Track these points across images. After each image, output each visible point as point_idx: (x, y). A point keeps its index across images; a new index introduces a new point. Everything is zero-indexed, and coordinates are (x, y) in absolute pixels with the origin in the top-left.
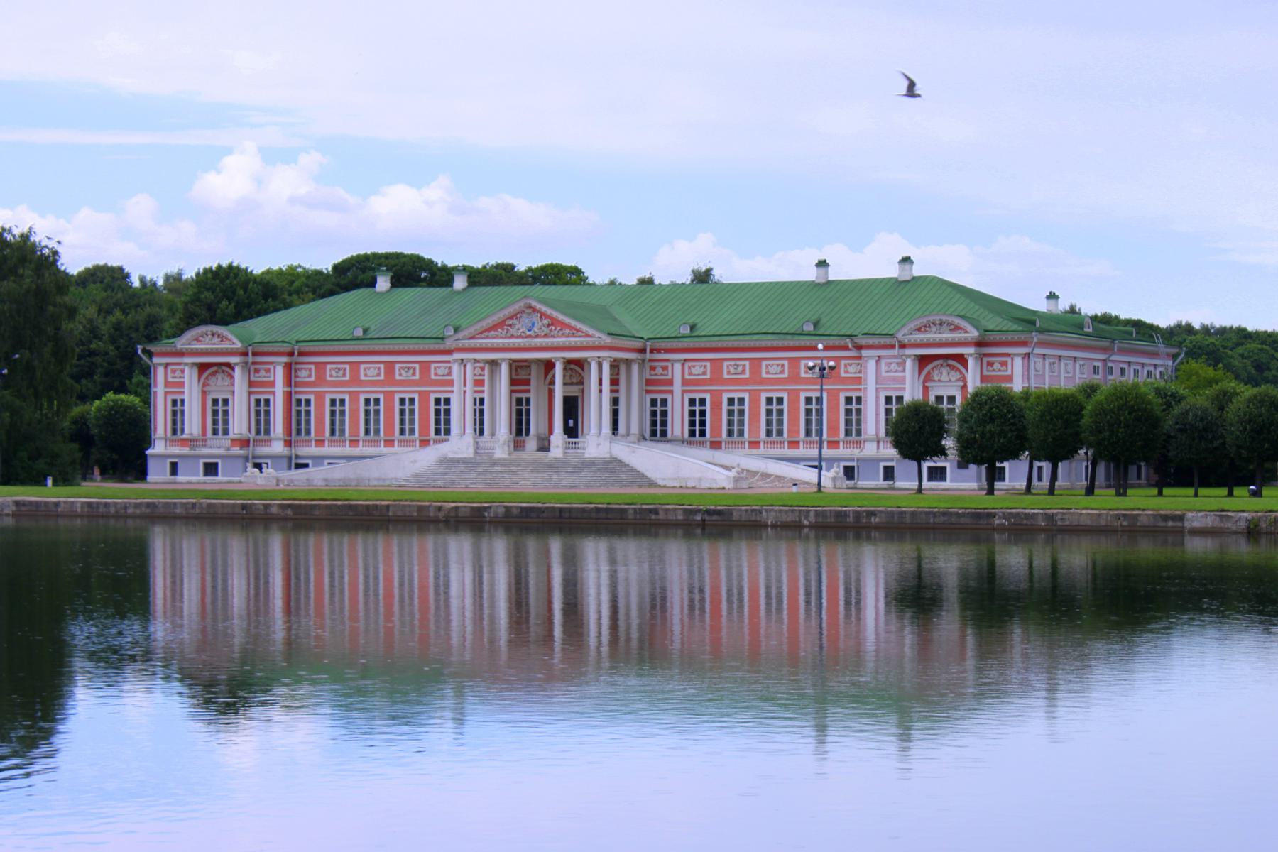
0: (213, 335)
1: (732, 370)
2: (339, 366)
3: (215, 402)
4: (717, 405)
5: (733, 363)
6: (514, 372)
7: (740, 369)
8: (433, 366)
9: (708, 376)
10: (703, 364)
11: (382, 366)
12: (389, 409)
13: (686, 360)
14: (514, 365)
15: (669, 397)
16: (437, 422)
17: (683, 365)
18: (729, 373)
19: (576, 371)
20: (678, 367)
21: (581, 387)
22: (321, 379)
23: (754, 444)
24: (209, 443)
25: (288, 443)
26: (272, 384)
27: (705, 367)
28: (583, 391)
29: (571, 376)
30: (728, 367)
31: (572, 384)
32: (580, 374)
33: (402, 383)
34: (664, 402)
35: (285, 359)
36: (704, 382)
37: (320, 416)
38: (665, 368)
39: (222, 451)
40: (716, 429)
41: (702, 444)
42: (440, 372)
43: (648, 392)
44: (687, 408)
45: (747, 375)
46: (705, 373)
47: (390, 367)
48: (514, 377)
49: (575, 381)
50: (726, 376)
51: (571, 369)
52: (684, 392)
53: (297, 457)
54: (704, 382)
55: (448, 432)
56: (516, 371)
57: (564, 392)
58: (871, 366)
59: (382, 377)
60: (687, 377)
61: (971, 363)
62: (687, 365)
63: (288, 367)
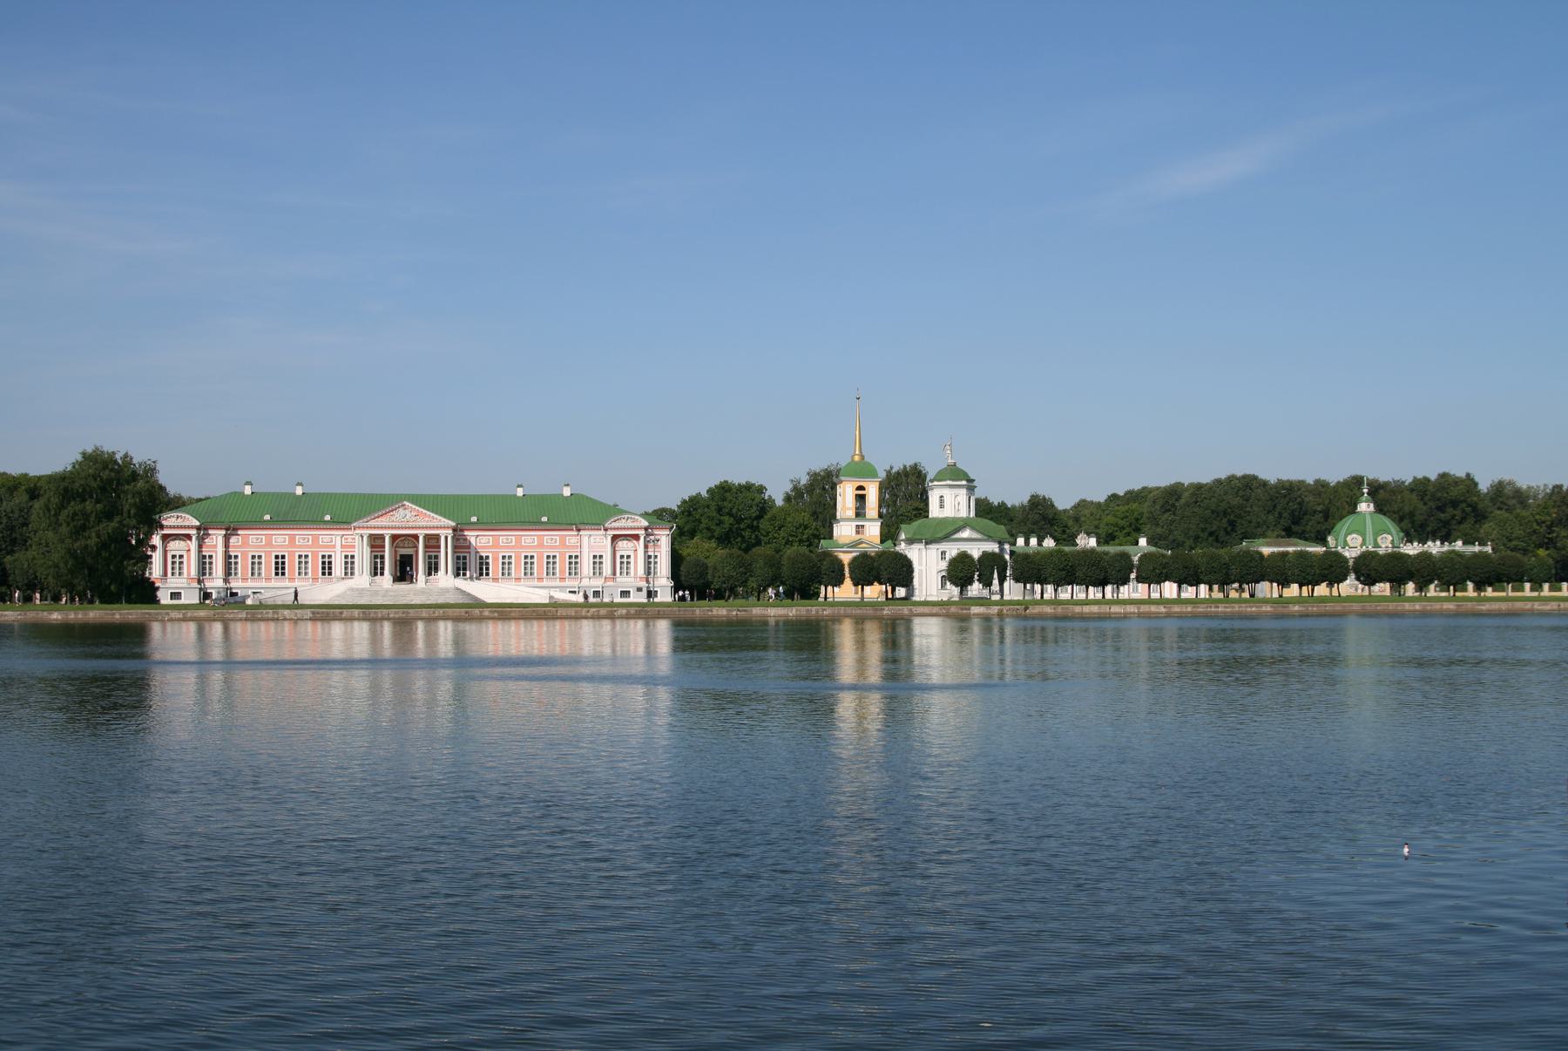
0: (178, 518)
1: (505, 541)
3: (174, 557)
4: (496, 559)
8: (321, 537)
9: (491, 544)
11: (287, 537)
12: (291, 561)
15: (468, 555)
16: (323, 568)
22: (245, 544)
23: (518, 579)
24: (168, 580)
25: (226, 581)
26: (215, 546)
33: (299, 546)
34: (465, 558)
35: (223, 532)
37: (242, 566)
39: (185, 585)
40: (495, 572)
43: (456, 552)
44: (478, 561)
47: (292, 538)
53: (231, 589)
55: (352, 574)
58: (585, 539)
59: (287, 543)
63: (227, 538)
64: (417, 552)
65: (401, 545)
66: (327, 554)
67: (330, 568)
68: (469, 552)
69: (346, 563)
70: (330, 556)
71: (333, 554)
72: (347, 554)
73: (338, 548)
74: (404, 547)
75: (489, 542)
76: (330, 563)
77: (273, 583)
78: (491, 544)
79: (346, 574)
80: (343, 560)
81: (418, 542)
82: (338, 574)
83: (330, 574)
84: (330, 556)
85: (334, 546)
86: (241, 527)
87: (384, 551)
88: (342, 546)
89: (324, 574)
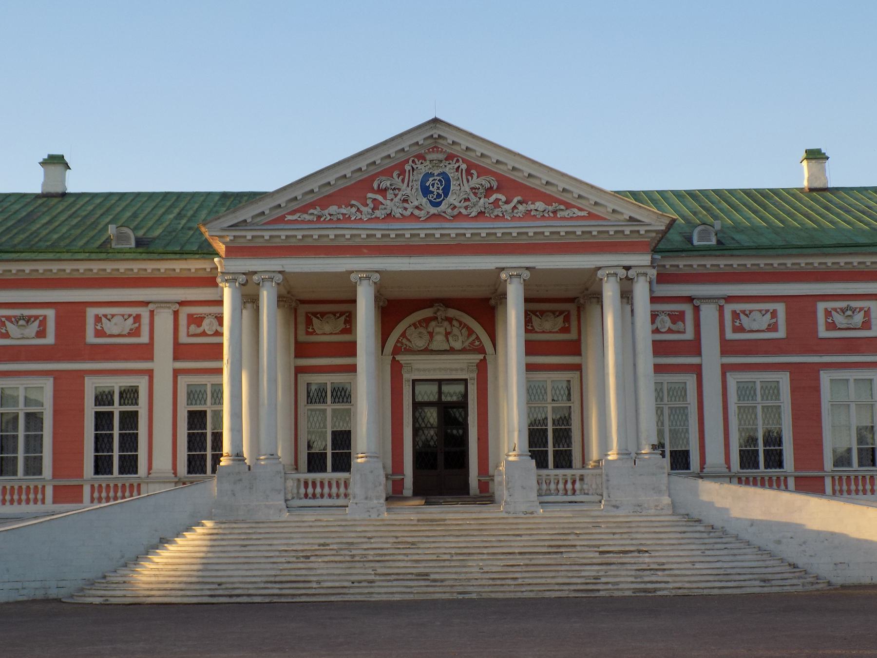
1: (839, 319)
6: (302, 328)
7: (859, 318)
9: (781, 333)
10: (771, 306)
13: (729, 299)
14: (303, 309)
16: (102, 442)
17: (721, 309)
18: (831, 326)
20: (709, 313)
27: (774, 314)
28: (482, 368)
29: (447, 334)
30: (828, 313)
31: (452, 351)
32: (471, 332)
36: (775, 347)
38: (677, 317)
41: (778, 484)
42: (109, 327)
46: (773, 328)
48: (303, 338)
49: (458, 345)
50: (823, 333)
51: (450, 320)
52: (726, 369)
54: (775, 347)
56: (309, 322)
57: (356, 375)
60: (730, 335)
62: (729, 308)
65: (420, 343)
66: (117, 384)
67: (130, 442)
68: (697, 370)
70: (129, 395)
71: (142, 383)
74: (427, 351)
75: (773, 328)
76: (130, 420)
78: (781, 333)
82: (163, 462)
83: (129, 465)
85: (146, 352)
88: (180, 351)
89: (102, 466)
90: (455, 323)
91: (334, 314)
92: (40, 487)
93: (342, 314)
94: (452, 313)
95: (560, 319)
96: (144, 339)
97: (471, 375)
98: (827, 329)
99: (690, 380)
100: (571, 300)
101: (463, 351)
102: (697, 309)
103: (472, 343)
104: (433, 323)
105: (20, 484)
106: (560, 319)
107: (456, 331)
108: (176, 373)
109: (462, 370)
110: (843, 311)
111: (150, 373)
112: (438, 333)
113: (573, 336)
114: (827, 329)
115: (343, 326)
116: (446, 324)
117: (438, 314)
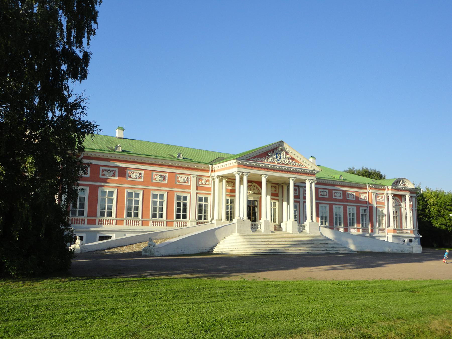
1: (322, 193)
2: (111, 169)
5: (323, 190)
11: (143, 172)
16: (178, 210)
19: (257, 188)
21: (259, 196)
29: (254, 189)
32: (258, 189)
33: (157, 184)
45: (327, 197)
49: (256, 192)
51: (255, 186)
61: (407, 198)
64: (261, 198)
67: (185, 211)
69: (200, 206)
72: (179, 194)
73: (193, 190)
77: (124, 227)
79: (200, 218)
80: (198, 203)
81: (261, 187)
83: (184, 217)
84: (185, 198)
85: (189, 187)
86: (113, 158)
87: (234, 196)
89: (178, 217)
90: (255, 187)
91: (231, 182)
92: (83, 219)
93: (233, 182)
94: (255, 184)
95: (275, 188)
96: (189, 184)
97: (258, 200)
98: (320, 195)
99: (297, 204)
100: (277, 184)
101: (257, 194)
102: (299, 189)
103: (259, 192)
104: (251, 186)
105: (77, 218)
106: (275, 188)
107: (256, 189)
108: (197, 193)
109: (256, 198)
110: (323, 192)
111: (190, 193)
112: (252, 189)
113: (277, 192)
114: (320, 195)
115: (233, 185)
116: (254, 187)
117: (253, 184)
